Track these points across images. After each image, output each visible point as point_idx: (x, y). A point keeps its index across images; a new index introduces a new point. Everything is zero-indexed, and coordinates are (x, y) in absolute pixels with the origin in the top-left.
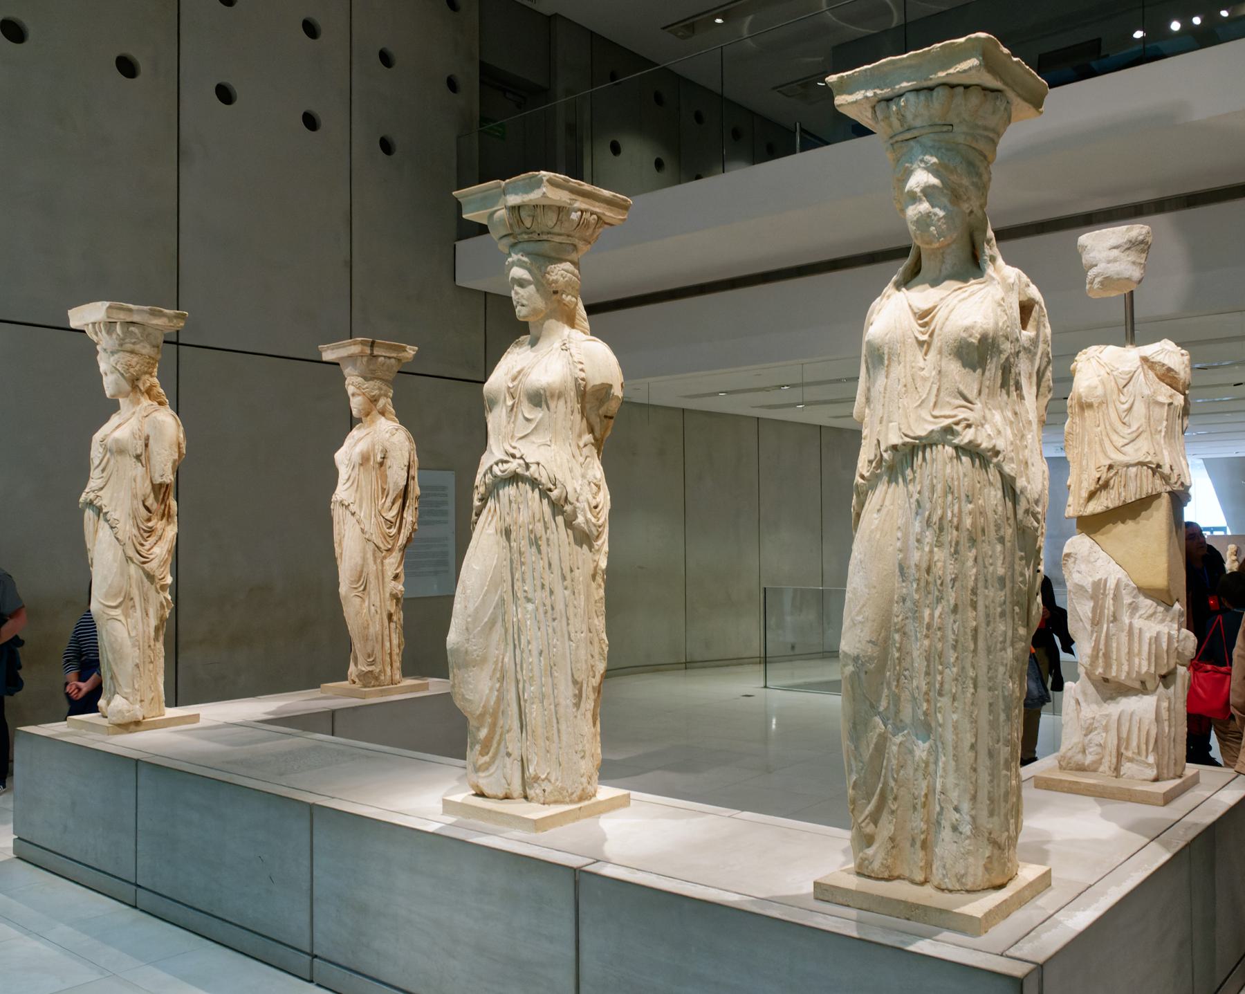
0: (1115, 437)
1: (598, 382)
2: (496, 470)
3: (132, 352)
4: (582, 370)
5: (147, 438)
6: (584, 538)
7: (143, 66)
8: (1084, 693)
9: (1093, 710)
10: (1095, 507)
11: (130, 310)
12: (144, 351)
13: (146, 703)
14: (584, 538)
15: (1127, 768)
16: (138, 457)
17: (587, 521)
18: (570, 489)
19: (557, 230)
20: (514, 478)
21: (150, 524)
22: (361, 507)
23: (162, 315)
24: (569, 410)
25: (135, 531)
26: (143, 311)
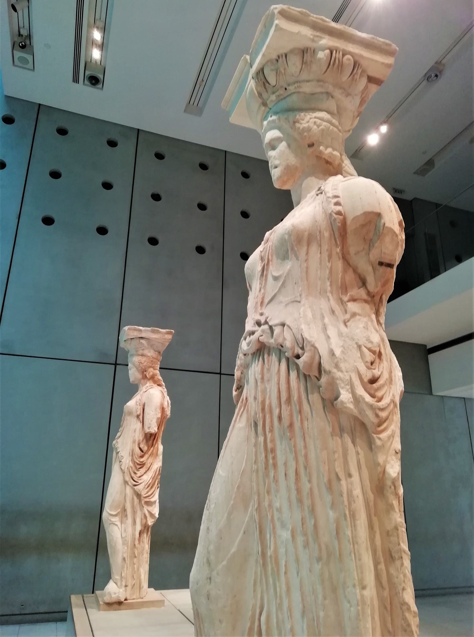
1: (359, 212)
3: (142, 355)
4: (337, 204)
5: (144, 406)
6: (362, 429)
7: (207, 249)
11: (140, 330)
12: (149, 354)
13: (129, 588)
14: (362, 429)
16: (138, 416)
17: (357, 400)
18: (323, 351)
19: (304, 76)
20: (261, 350)
21: (142, 460)
23: (158, 332)
24: (325, 255)
25: (131, 464)
26: (147, 330)
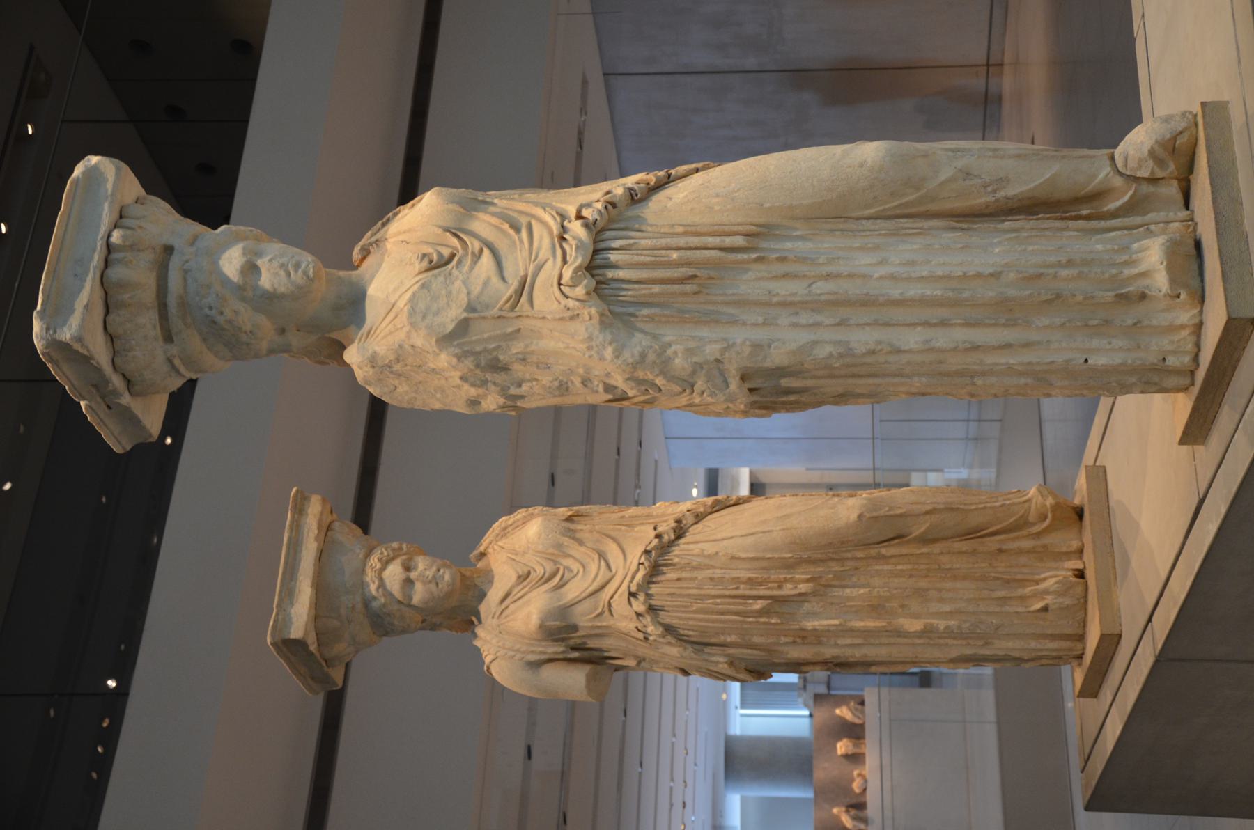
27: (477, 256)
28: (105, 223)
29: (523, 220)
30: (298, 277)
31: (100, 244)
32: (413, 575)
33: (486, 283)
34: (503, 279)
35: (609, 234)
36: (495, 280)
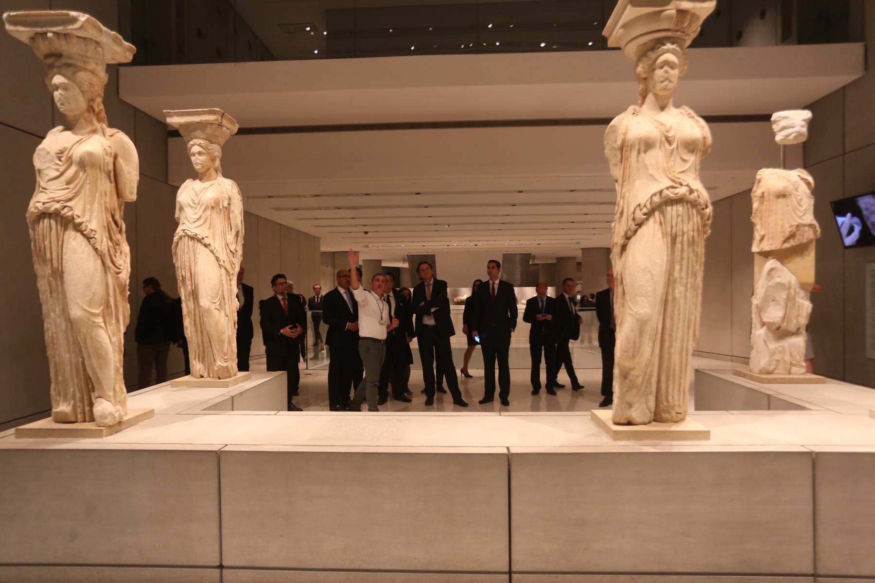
0: (797, 212)
2: (666, 192)
8: (767, 336)
9: (773, 345)
10: (787, 245)
15: (794, 369)
22: (214, 240)
27: (57, 170)
28: (55, 29)
29: (71, 186)
30: (59, 106)
31: (44, 29)
32: (197, 156)
33: (47, 175)
34: (49, 181)
35: (59, 219)
36: (47, 178)
